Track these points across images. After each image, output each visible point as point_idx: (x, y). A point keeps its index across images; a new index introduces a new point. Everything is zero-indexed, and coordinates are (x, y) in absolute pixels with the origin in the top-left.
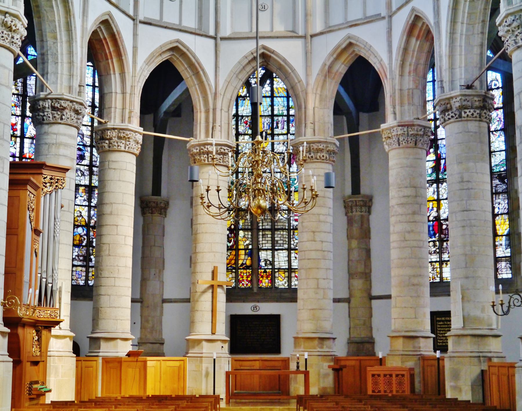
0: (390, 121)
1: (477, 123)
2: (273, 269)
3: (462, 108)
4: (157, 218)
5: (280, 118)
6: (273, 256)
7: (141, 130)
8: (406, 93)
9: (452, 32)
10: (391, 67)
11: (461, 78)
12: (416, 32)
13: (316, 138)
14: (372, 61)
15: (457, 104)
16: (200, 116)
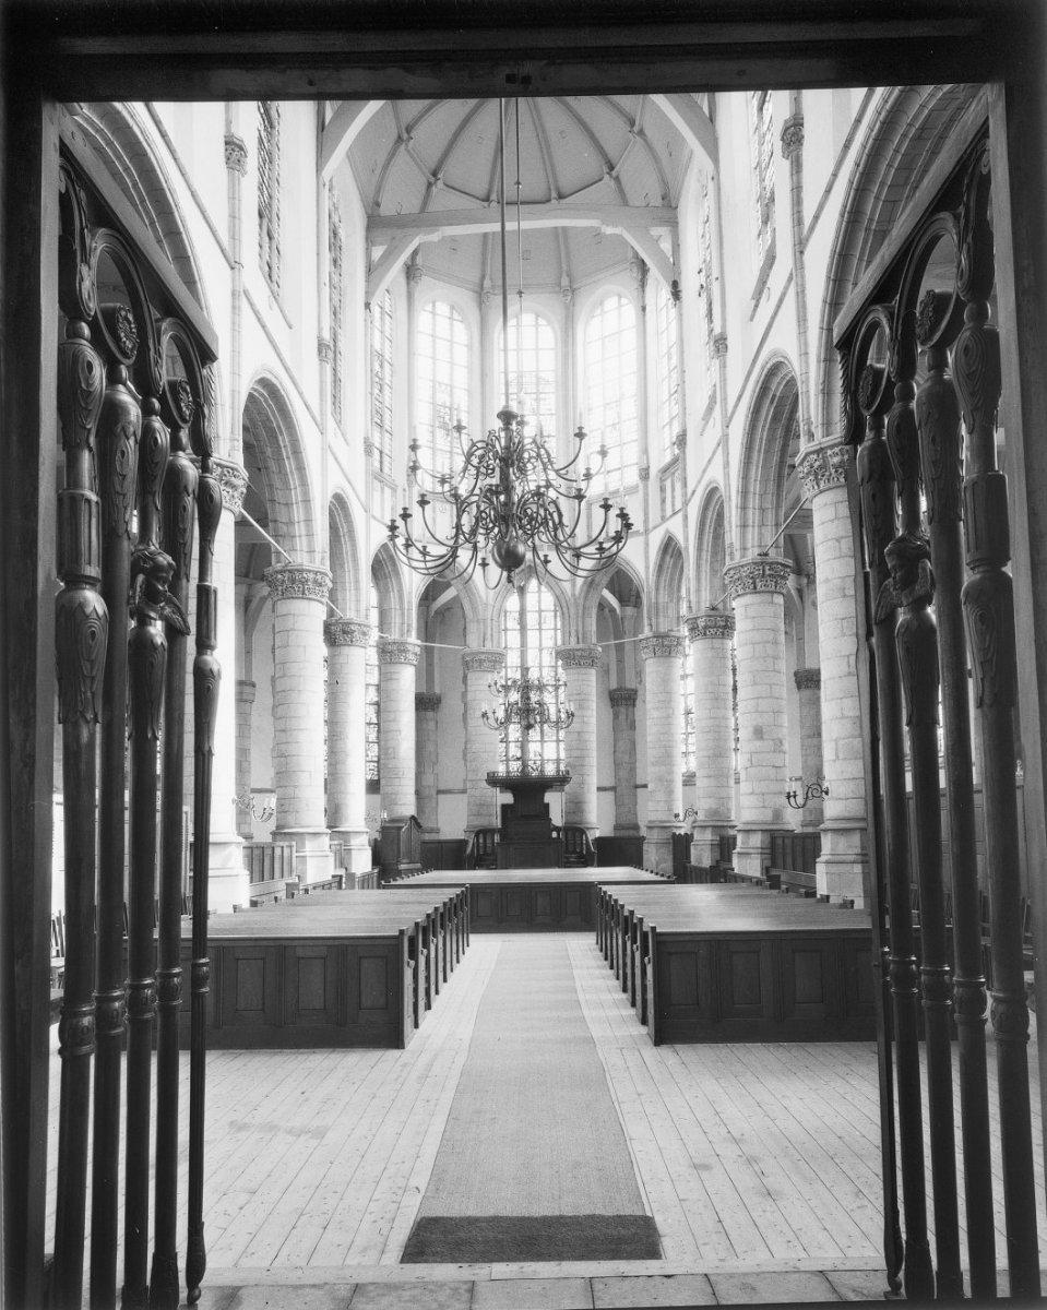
0: (647, 632)
1: (720, 641)
2: (542, 760)
3: (705, 627)
4: (430, 714)
5: (548, 614)
6: (542, 748)
7: (419, 642)
8: (661, 607)
9: (699, 558)
10: (647, 578)
11: (705, 604)
12: (670, 551)
13: (581, 646)
14: (631, 573)
15: (703, 624)
16: (472, 628)
